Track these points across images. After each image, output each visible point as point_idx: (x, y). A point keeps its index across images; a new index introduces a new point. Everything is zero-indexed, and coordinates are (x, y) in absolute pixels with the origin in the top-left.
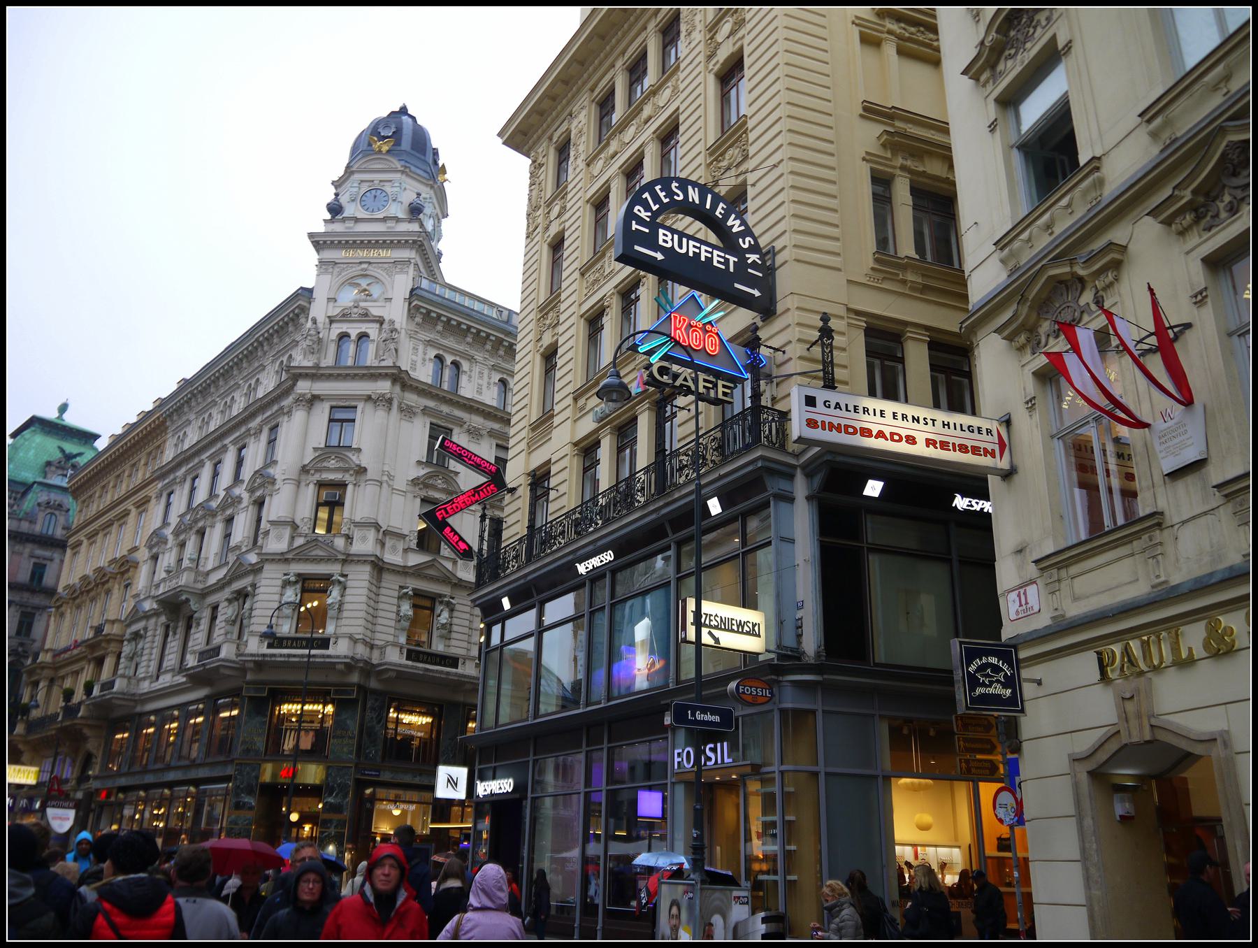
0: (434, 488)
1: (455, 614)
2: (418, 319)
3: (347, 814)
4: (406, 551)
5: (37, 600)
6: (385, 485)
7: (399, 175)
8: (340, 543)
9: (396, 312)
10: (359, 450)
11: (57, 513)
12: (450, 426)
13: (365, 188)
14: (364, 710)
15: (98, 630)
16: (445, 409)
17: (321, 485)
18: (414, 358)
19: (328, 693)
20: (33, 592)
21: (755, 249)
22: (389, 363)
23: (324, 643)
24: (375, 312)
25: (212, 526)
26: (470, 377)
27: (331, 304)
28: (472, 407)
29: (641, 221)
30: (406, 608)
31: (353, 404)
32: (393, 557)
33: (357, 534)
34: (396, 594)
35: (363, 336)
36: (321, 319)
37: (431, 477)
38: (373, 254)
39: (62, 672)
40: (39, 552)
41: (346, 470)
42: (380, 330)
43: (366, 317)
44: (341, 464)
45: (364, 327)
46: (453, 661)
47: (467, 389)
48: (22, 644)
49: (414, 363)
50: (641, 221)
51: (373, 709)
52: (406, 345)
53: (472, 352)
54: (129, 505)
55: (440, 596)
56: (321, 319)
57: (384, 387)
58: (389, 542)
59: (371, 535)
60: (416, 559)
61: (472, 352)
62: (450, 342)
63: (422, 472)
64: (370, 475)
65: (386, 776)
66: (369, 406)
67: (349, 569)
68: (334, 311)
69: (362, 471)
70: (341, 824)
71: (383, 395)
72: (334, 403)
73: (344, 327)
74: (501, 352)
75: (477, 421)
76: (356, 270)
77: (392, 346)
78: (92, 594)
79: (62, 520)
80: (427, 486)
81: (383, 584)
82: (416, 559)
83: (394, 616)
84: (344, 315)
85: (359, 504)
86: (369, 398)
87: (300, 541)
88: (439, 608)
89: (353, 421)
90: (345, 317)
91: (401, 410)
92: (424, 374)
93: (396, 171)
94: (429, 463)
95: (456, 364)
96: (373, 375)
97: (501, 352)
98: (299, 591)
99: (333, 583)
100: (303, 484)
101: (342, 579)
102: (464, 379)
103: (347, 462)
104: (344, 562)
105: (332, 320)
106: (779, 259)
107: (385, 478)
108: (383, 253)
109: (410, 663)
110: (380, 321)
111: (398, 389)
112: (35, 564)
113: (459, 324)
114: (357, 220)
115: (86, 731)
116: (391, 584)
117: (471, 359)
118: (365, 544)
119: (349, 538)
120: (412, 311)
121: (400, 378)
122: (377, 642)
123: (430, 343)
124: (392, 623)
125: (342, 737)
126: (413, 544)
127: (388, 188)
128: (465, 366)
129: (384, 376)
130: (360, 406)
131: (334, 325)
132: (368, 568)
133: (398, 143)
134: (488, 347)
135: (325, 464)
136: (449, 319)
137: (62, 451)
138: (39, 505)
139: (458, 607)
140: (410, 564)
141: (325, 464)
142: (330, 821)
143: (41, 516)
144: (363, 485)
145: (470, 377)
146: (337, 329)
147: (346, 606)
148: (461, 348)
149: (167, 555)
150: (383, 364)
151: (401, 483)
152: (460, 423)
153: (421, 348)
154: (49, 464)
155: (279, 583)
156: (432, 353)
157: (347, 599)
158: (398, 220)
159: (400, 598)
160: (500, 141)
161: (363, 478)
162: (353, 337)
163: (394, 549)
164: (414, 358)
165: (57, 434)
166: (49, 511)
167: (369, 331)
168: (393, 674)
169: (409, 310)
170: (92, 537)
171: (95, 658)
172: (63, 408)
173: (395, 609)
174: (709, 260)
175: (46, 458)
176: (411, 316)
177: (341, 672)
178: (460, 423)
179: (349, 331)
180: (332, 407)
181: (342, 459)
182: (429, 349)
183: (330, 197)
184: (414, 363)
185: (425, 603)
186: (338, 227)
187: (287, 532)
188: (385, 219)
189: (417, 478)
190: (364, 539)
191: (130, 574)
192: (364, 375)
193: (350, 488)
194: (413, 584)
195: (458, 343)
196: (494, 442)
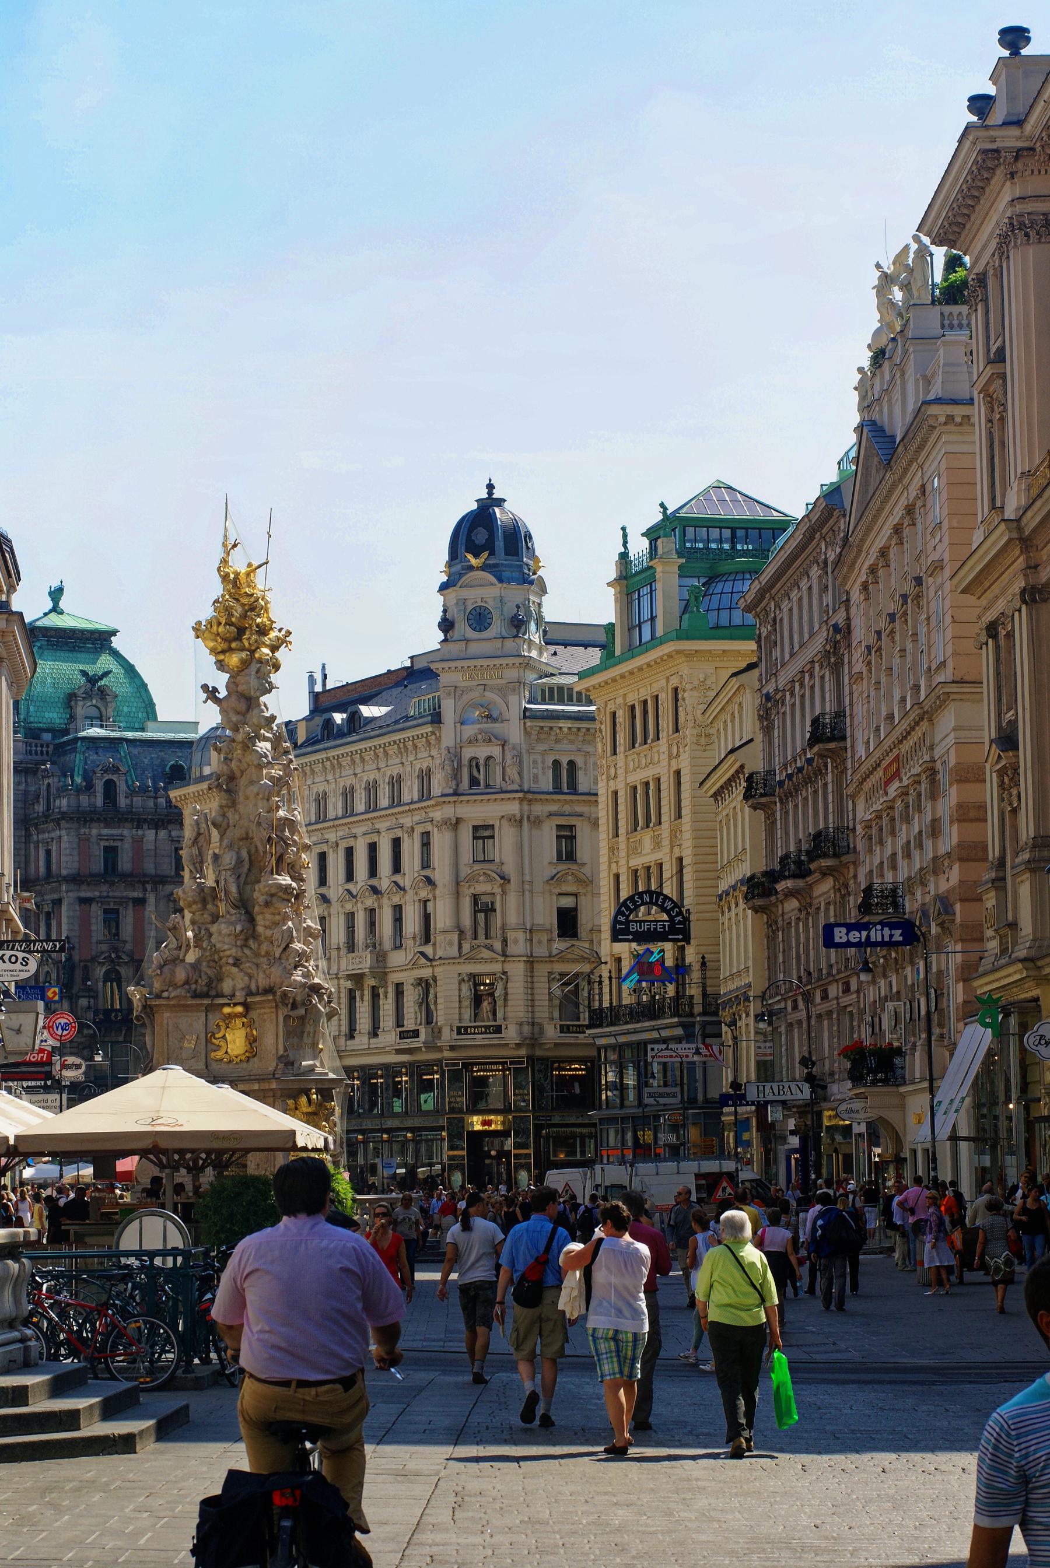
5: (120, 891)
17: (475, 898)
21: (680, 913)
23: (498, 1029)
25: (380, 907)
26: (586, 770)
29: (621, 923)
35: (488, 758)
50: (621, 923)
65: (556, 1120)
89: (492, 837)
90: (472, 741)
95: (572, 764)
106: (692, 917)
112: (105, 847)
128: (580, 761)
147: (510, 997)
155: (456, 982)
163: (540, 942)
174: (655, 929)
186: (454, 648)
190: (516, 942)
193: (498, 898)
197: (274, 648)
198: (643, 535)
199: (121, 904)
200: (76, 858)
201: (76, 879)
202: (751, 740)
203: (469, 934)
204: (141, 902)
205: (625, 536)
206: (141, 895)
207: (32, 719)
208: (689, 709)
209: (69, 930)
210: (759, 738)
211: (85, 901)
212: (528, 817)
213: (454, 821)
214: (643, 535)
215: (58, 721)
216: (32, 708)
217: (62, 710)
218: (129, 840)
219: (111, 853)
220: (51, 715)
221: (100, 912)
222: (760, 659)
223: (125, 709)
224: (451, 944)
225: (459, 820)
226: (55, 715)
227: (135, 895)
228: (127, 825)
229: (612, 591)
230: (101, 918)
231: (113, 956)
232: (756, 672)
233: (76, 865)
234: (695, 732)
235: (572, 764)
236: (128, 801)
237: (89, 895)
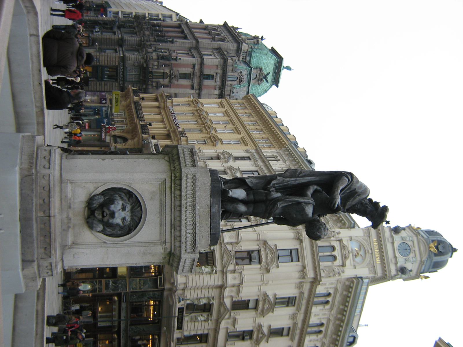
0: (264, 304)
1: (203, 323)
2: (347, 283)
3: (104, 292)
4: (232, 297)
5: (196, 79)
6: (262, 283)
7: (418, 258)
8: (231, 267)
9: (349, 272)
10: (278, 267)
11: (238, 80)
12: (296, 305)
13: (410, 243)
14: (153, 291)
15: (182, 133)
16: (304, 302)
18: (328, 284)
19: (160, 274)
20: (200, 77)
22: (323, 274)
24: (348, 262)
27: (348, 239)
28: (307, 314)
30: (203, 302)
31: (300, 260)
32: (227, 292)
33: (236, 275)
34: (210, 295)
35: (335, 258)
36: (340, 236)
37: (269, 302)
38: (377, 254)
39: (163, 112)
40: (219, 76)
41: (267, 263)
42: (339, 266)
43: (344, 258)
44: (269, 260)
45: (339, 258)
46: (180, 327)
47: (315, 310)
48: (175, 76)
49: (325, 284)
51: (154, 295)
52: (333, 279)
53: (335, 309)
54: (243, 134)
55: (211, 315)
56: (340, 236)
57: (310, 274)
58: (234, 289)
59: (237, 282)
60: (228, 302)
61: (335, 309)
62: (338, 298)
63: (271, 298)
64: (266, 276)
65: (123, 305)
66: (300, 268)
67: (219, 274)
68: (345, 242)
69: (268, 271)
70: (100, 290)
71: (306, 275)
72: (299, 250)
73: (338, 248)
74: (337, 322)
75: (300, 317)
76: (367, 247)
77: (331, 274)
78: (199, 120)
79: (235, 83)
80: (264, 301)
81: (214, 290)
82: (228, 302)
83: (199, 296)
84: (344, 247)
85: (251, 271)
86: (304, 267)
87: (229, 247)
88: (205, 314)
89: (292, 261)
90: (343, 247)
91: (300, 283)
92: (320, 289)
93: (421, 257)
96: (316, 268)
97: (337, 322)
98: (207, 251)
99: (212, 267)
100: (258, 242)
101: (214, 272)
102: (320, 307)
103: (271, 263)
104: (223, 271)
105: (340, 241)
107: (265, 282)
108: (378, 260)
109: (177, 309)
110: (343, 265)
113: (348, 302)
114: (393, 243)
115: (136, 139)
116: (215, 293)
117: (332, 308)
118: (231, 279)
119: (234, 271)
120: (350, 280)
121: (316, 281)
122: (186, 291)
123: (336, 289)
124: (196, 296)
125: (140, 283)
126: (234, 299)
127: (412, 255)
128: (328, 307)
129: (315, 272)
130: (300, 263)
131: (338, 242)
132: (220, 283)
133: (436, 255)
134: (339, 316)
135: (269, 252)
136: (349, 297)
137: (268, 74)
138: (241, 72)
139: (207, 323)
140: (225, 300)
141: (269, 252)
142: (101, 285)
143: (236, 74)
144: (261, 272)
145: (323, 310)
146: (336, 244)
147: (201, 276)
148: (336, 303)
149: (219, 164)
151: (264, 289)
152: (298, 309)
153: (333, 286)
154: (261, 69)
157: (205, 276)
158: (396, 264)
159: (208, 298)
160: (437, 339)
161: (264, 271)
162: (334, 253)
163: (232, 291)
164: (328, 284)
165: (276, 69)
166: (238, 77)
167: (338, 261)
168: (171, 303)
169: (351, 278)
170: (226, 113)
171: (170, 133)
172: (288, 68)
173: (203, 296)
175: (263, 67)
176: (348, 279)
177: (170, 280)
178: (298, 309)
179: (336, 251)
180: (297, 249)
181: (272, 260)
183: (402, 226)
184: (325, 284)
185: (207, 308)
187: (234, 240)
188: (395, 257)
189: (268, 296)
191: (210, 143)
192: (315, 263)
193: (259, 266)
194: (215, 303)
195: (339, 302)
196: (291, 326)
199: (193, 80)
200: (210, 64)
201: (202, 64)
203: (237, 249)
204: (192, 88)
206: (195, 88)
207: (254, 54)
209: (183, 60)
211: (194, 66)
212: (303, 282)
213: (301, 238)
215: (252, 64)
216: (258, 54)
217: (256, 65)
218: (216, 84)
219: (210, 77)
220: (255, 61)
221: (189, 72)
223: (254, 88)
224: (231, 237)
225: (301, 241)
226: (254, 63)
227: (195, 86)
228: (220, 84)
230: (187, 72)
231: (173, 76)
233: (207, 64)
237: (196, 68)
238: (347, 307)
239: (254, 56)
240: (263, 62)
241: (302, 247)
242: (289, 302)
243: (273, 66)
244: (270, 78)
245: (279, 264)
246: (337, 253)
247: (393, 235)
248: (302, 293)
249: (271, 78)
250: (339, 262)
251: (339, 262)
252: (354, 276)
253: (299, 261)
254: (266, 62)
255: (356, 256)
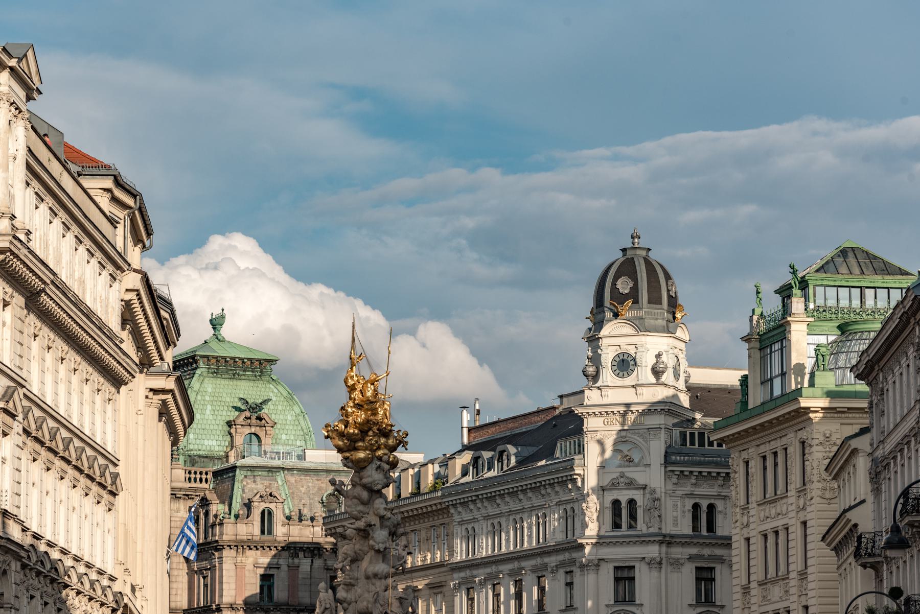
2: (674, 480)
12: (712, 565)
16: (707, 552)
18: (675, 514)
24: (641, 479)
26: (726, 514)
31: (632, 564)
35: (632, 502)
43: (631, 484)
49: (675, 520)
57: (653, 551)
62: (704, 489)
72: (617, 565)
77: (657, 513)
90: (614, 485)
94: (699, 603)
95: (711, 507)
96: (644, 540)
102: (719, 519)
110: (644, 488)
111: (664, 548)
113: (709, 473)
121: (668, 540)
130: (637, 565)
133: (636, 302)
146: (610, 497)
148: (714, 491)
150: (651, 530)
156: (689, 503)
164: (675, 514)
167: (635, 497)
169: (665, 472)
179: (620, 498)
180: (616, 568)
182: (687, 500)
195: (712, 486)
197: (393, 449)
198: (776, 292)
202: (863, 501)
205: (758, 292)
207: (191, 447)
208: (815, 464)
210: (870, 499)
213: (596, 562)
214: (776, 292)
215: (217, 448)
217: (221, 438)
218: (284, 568)
220: (210, 443)
222: (872, 424)
223: (284, 437)
226: (214, 443)
229: (746, 345)
232: (866, 438)
233: (233, 593)
234: (820, 485)
235: (711, 507)
236: (284, 530)
238: (718, 473)
239: (196, 447)
240: (211, 417)
241: (612, 560)
242: (705, 578)
243: (219, 381)
244: (251, 390)
245: (637, 602)
246: (624, 497)
247: (597, 385)
248: (691, 558)
249: (251, 384)
250: (637, 495)
251: (637, 495)
252: (663, 468)
253: (633, 567)
254: (209, 407)
255: (631, 460)
